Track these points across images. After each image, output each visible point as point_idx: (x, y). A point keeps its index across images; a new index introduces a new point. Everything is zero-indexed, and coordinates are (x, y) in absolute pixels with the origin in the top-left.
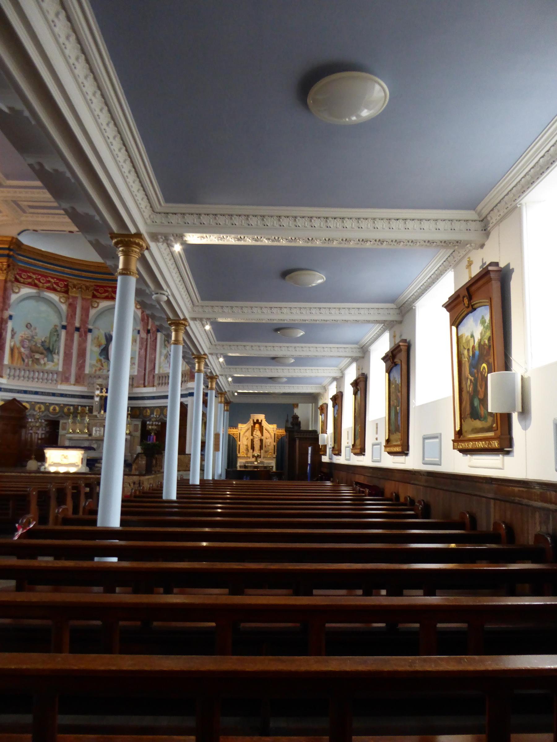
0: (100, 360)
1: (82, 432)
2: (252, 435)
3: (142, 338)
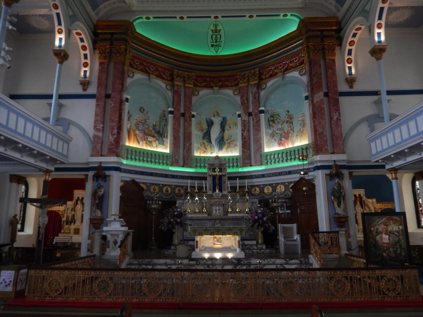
0: (204, 143)
1: (201, 212)
2: (355, 210)
3: (244, 121)
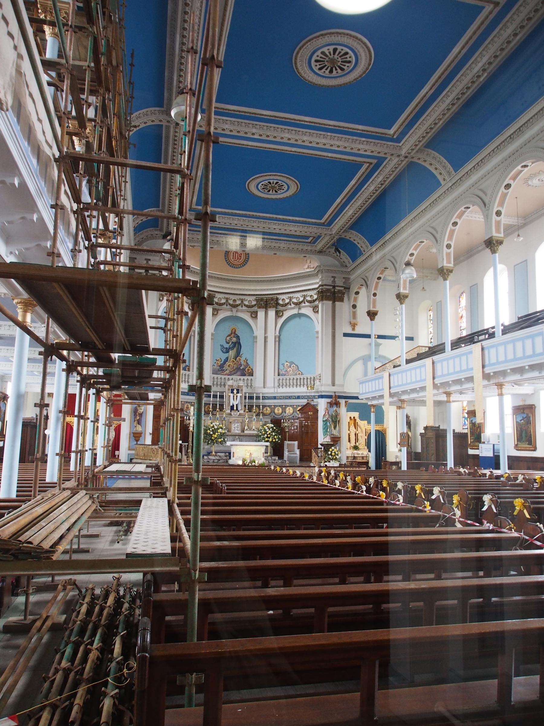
2: (349, 430)
